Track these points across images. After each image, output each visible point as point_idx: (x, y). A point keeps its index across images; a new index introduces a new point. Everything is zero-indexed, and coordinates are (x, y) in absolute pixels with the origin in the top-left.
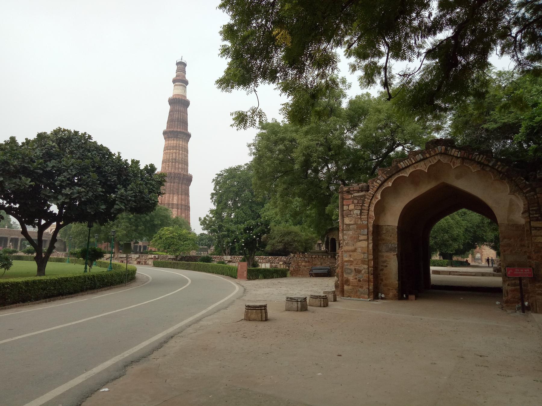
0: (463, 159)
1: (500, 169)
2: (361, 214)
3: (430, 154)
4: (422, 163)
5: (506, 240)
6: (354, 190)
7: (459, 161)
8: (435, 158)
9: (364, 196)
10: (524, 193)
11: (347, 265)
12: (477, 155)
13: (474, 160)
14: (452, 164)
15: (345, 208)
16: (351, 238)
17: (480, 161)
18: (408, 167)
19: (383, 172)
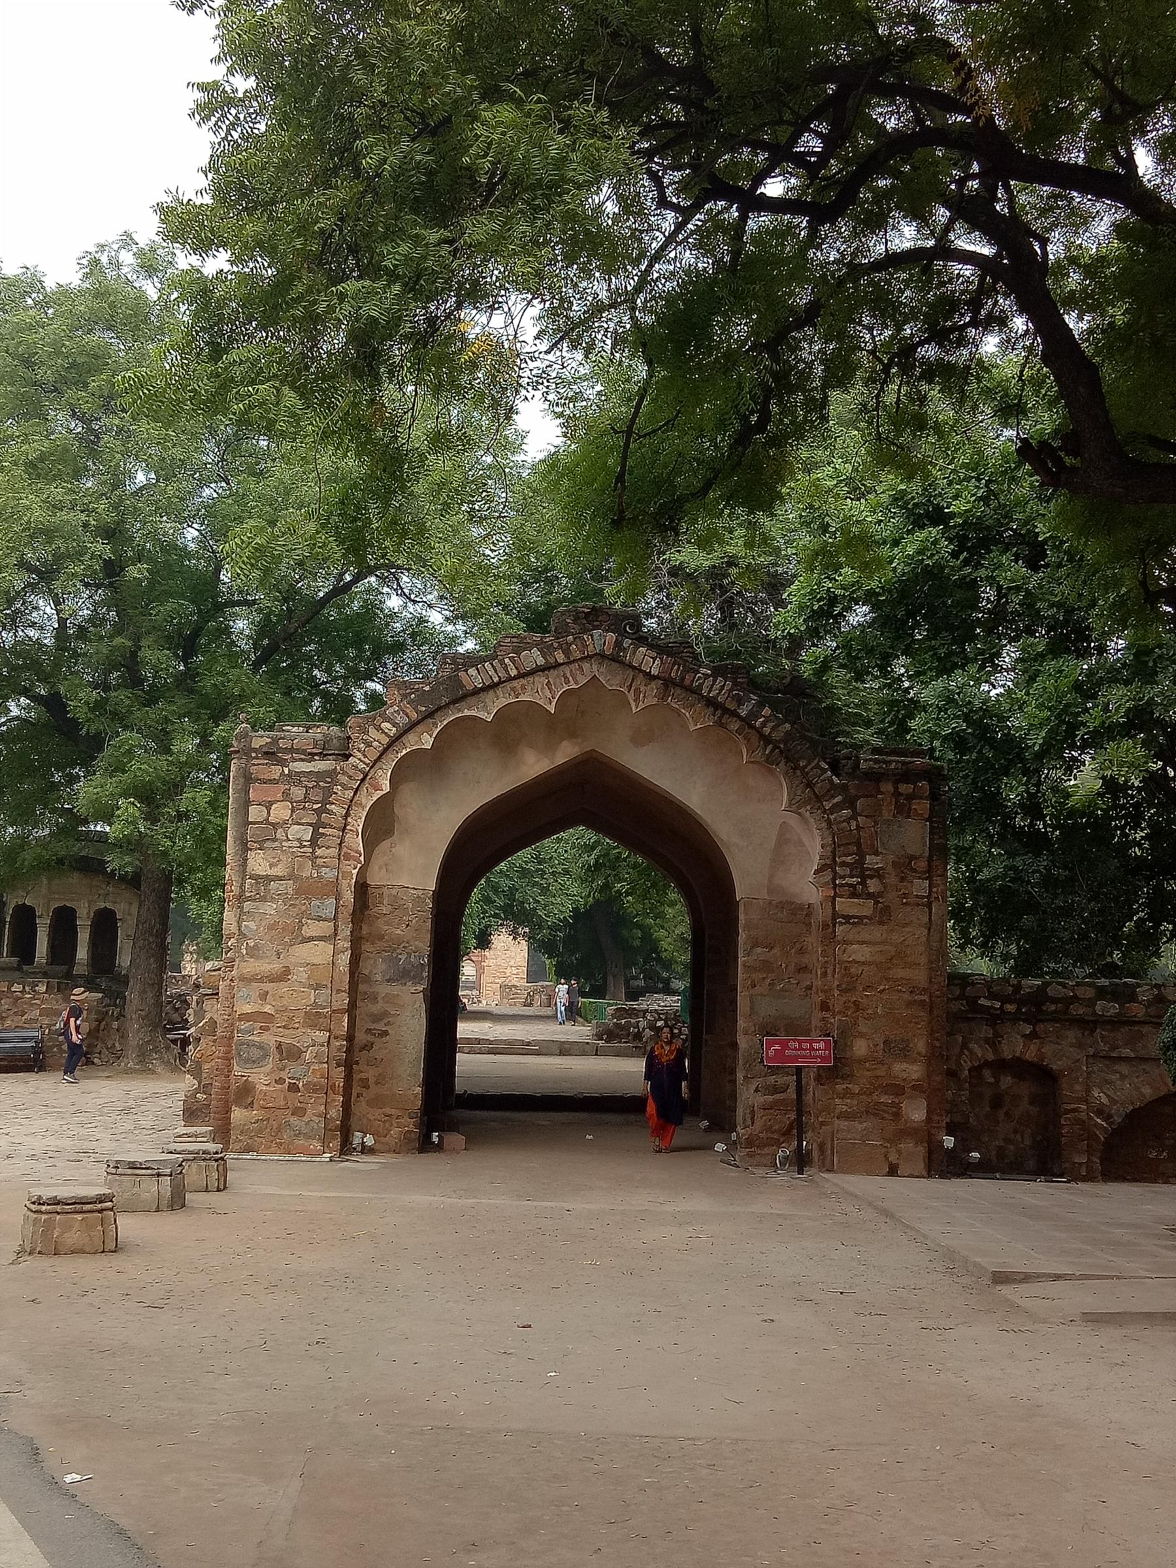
0: (668, 683)
1: (767, 730)
2: (314, 842)
3: (567, 652)
4: (540, 680)
5: (759, 950)
6: (292, 750)
7: (653, 685)
8: (581, 668)
9: (332, 774)
10: (825, 811)
11: (250, 1032)
12: (706, 676)
13: (696, 691)
14: (631, 697)
15: (255, 813)
16: (271, 928)
17: (715, 698)
18: (493, 686)
19: (404, 696)
